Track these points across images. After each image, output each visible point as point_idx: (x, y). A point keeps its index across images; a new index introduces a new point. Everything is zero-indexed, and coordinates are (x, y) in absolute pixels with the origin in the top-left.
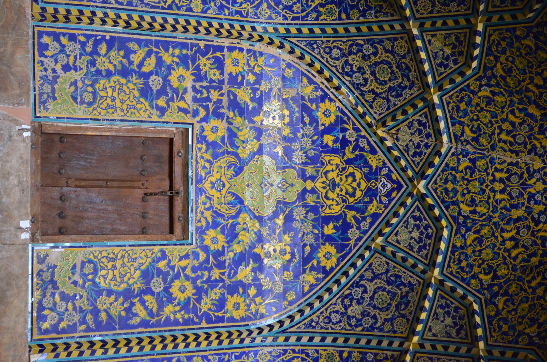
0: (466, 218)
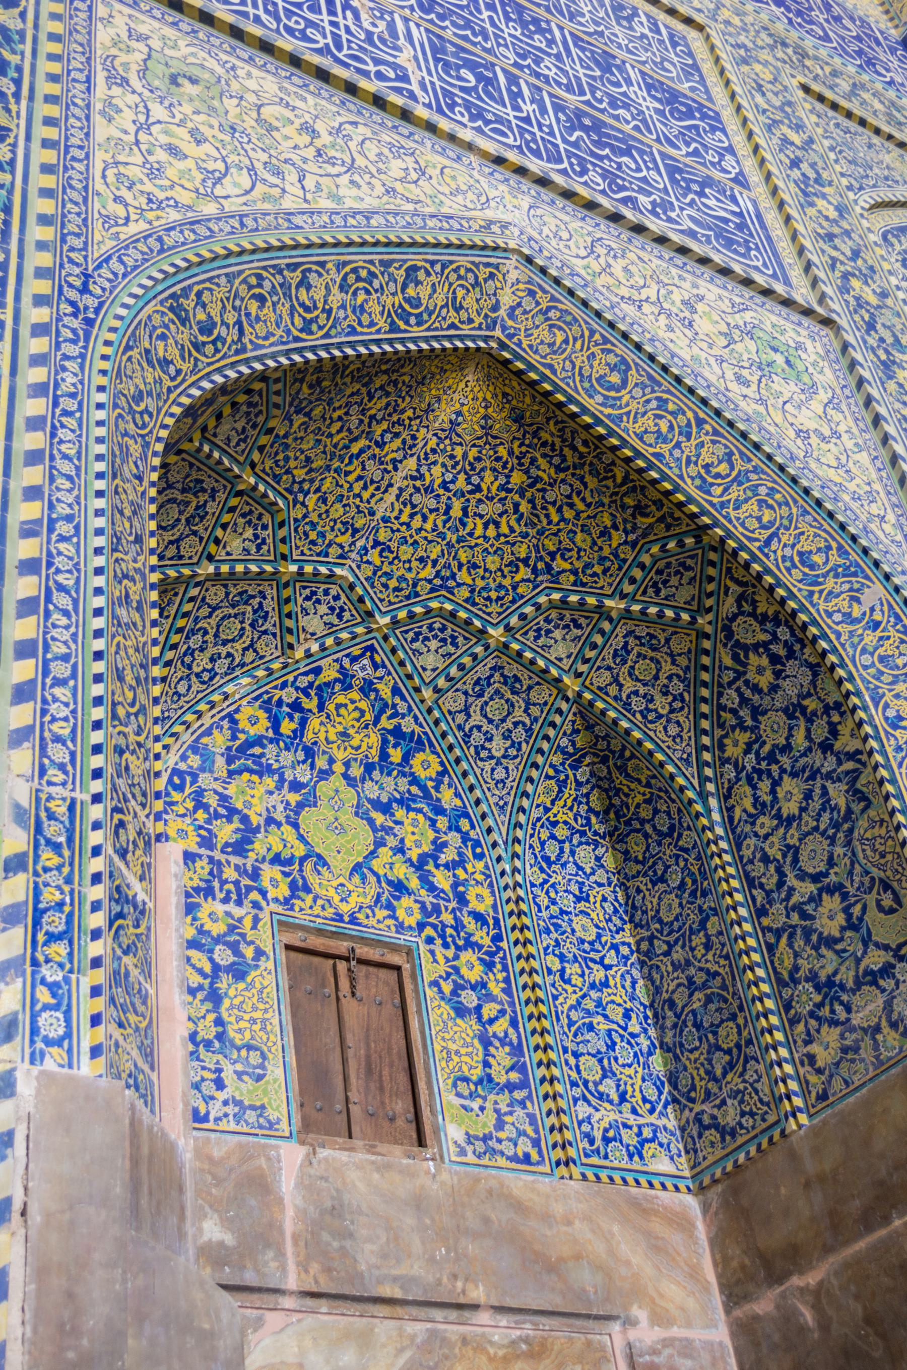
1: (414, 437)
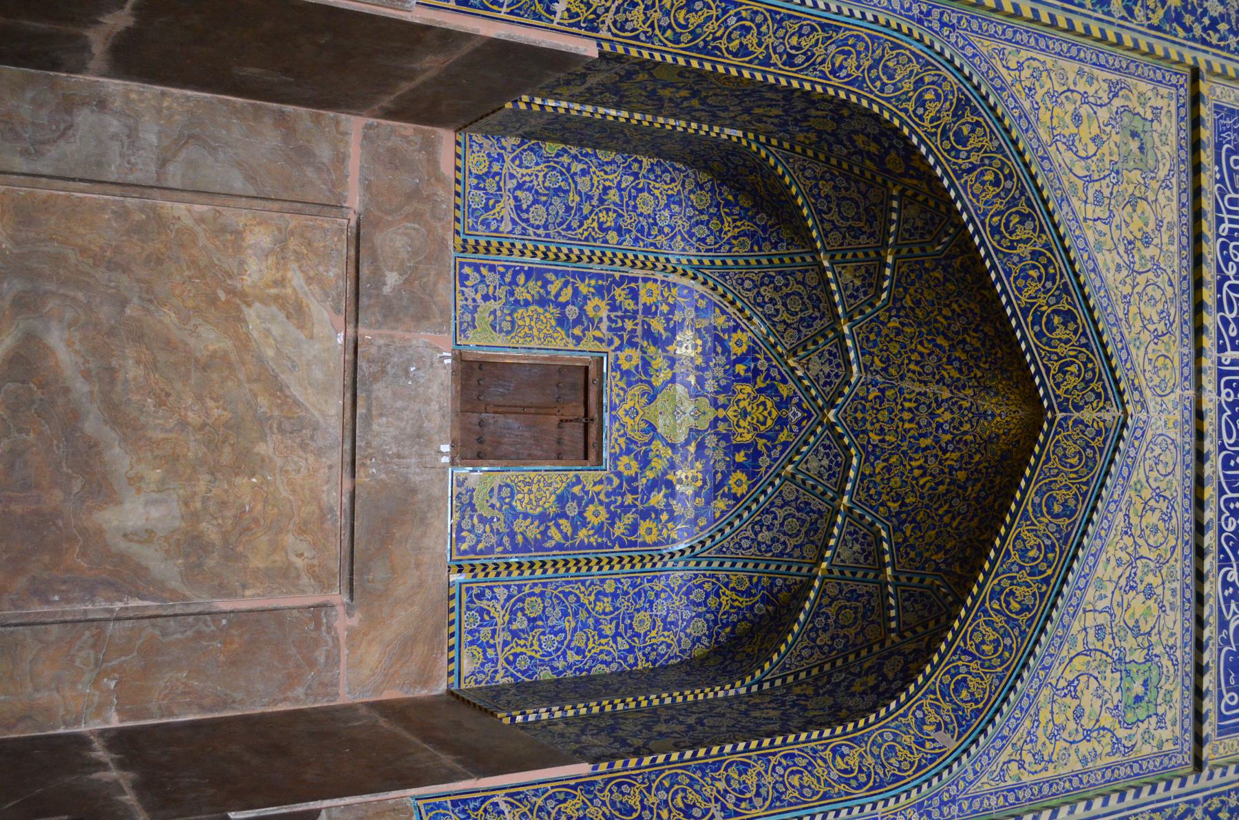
0: (875, 446)
1: (964, 387)
